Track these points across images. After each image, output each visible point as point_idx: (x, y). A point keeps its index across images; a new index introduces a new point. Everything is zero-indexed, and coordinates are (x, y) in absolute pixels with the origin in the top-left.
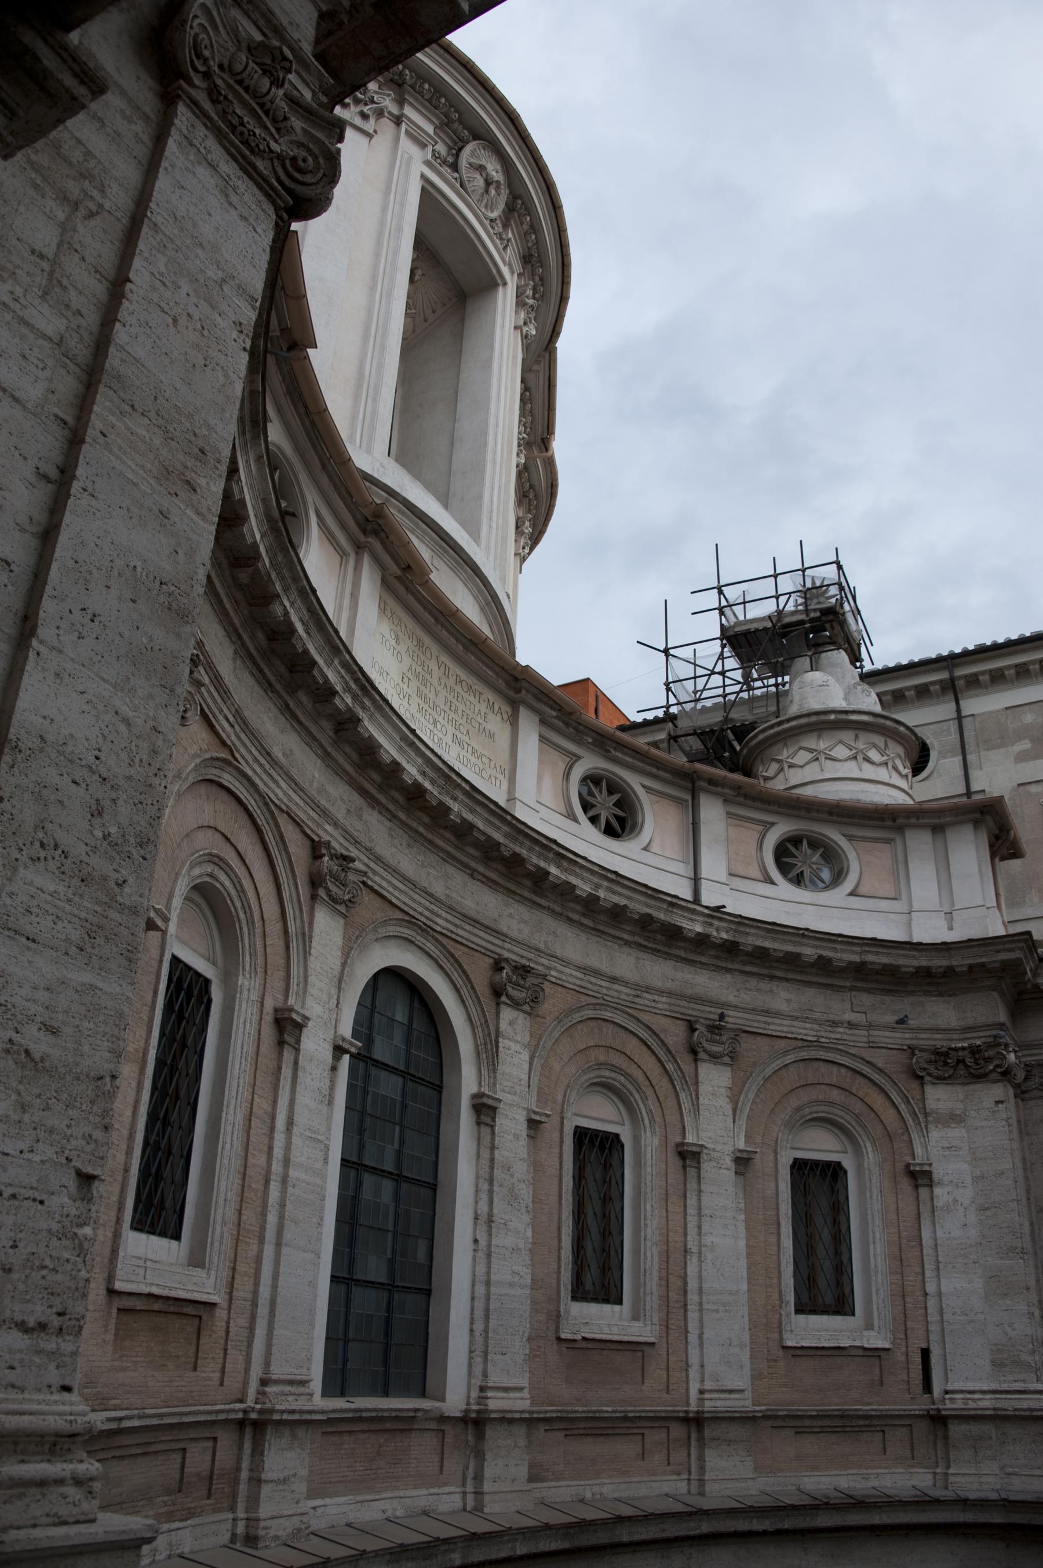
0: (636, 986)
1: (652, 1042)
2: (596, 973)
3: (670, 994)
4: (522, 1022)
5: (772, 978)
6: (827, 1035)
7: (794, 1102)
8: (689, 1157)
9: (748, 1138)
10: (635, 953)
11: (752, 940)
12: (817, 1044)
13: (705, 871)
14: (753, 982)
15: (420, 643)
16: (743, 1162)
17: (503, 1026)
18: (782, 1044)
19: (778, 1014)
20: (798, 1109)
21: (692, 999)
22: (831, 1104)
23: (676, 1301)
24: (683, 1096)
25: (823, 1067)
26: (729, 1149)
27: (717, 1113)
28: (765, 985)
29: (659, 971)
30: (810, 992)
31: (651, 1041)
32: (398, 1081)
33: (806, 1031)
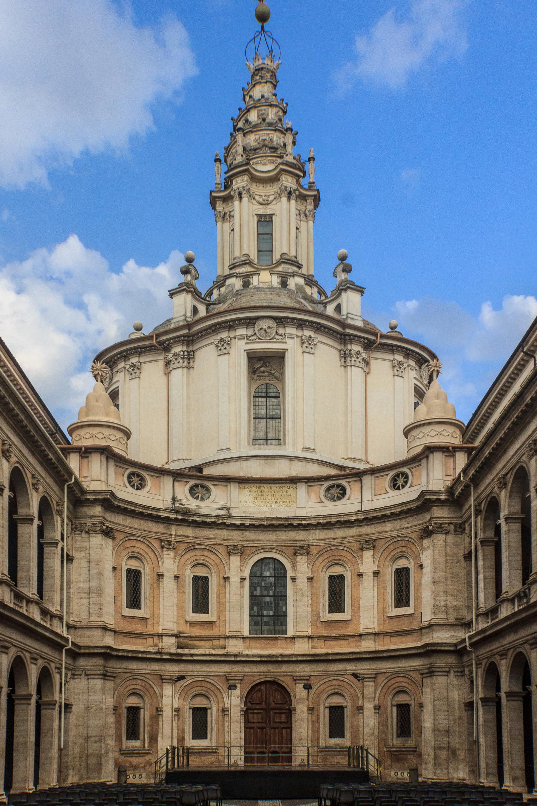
0: (342, 538)
1: (349, 550)
2: (328, 539)
3: (353, 536)
4: (304, 558)
5: (385, 522)
6: (400, 533)
7: (392, 554)
8: (360, 575)
9: (378, 566)
10: (343, 529)
11: (371, 515)
12: (398, 536)
13: (364, 498)
14: (380, 525)
15: (259, 487)
16: (376, 574)
17: (297, 560)
18: (389, 539)
19: (385, 532)
20: (393, 556)
21: (360, 536)
22: (402, 552)
23: (357, 610)
24: (359, 561)
25: (401, 542)
26: (371, 571)
27: (368, 562)
28: (383, 524)
29: (351, 532)
30: (396, 522)
31: (348, 550)
32: (273, 578)
33: (394, 534)
